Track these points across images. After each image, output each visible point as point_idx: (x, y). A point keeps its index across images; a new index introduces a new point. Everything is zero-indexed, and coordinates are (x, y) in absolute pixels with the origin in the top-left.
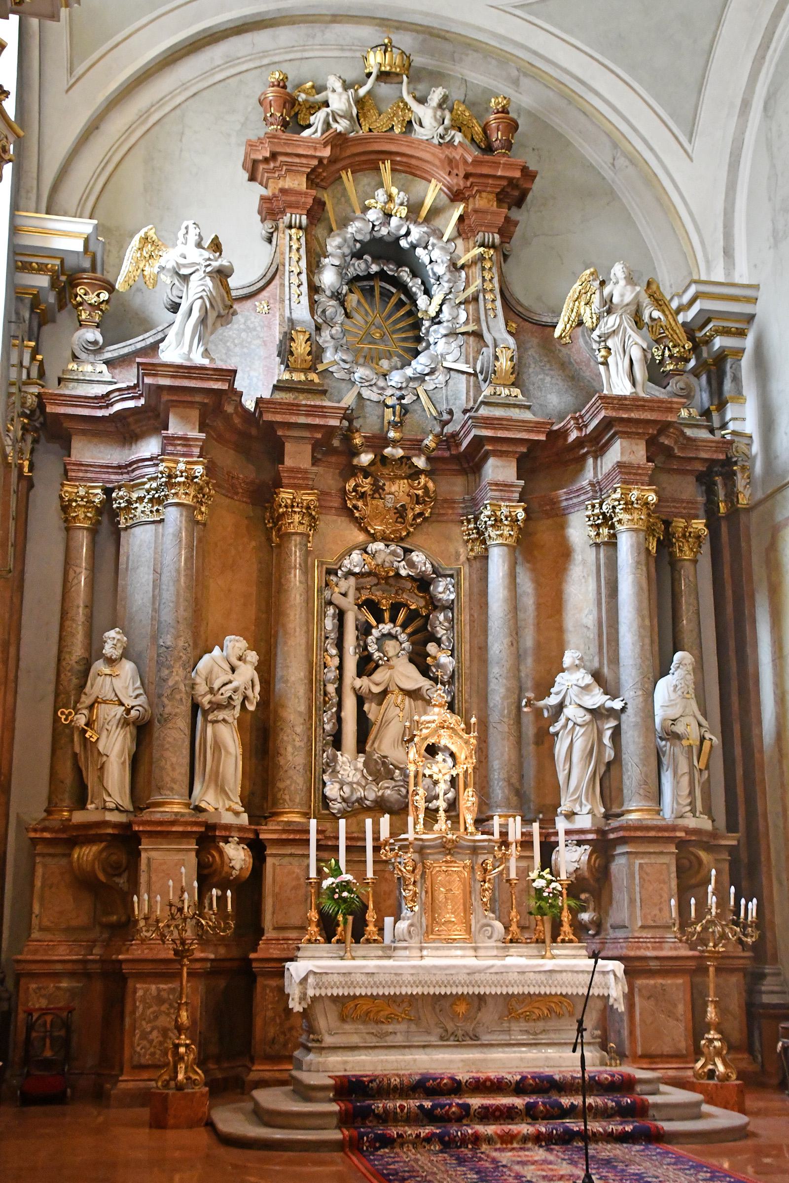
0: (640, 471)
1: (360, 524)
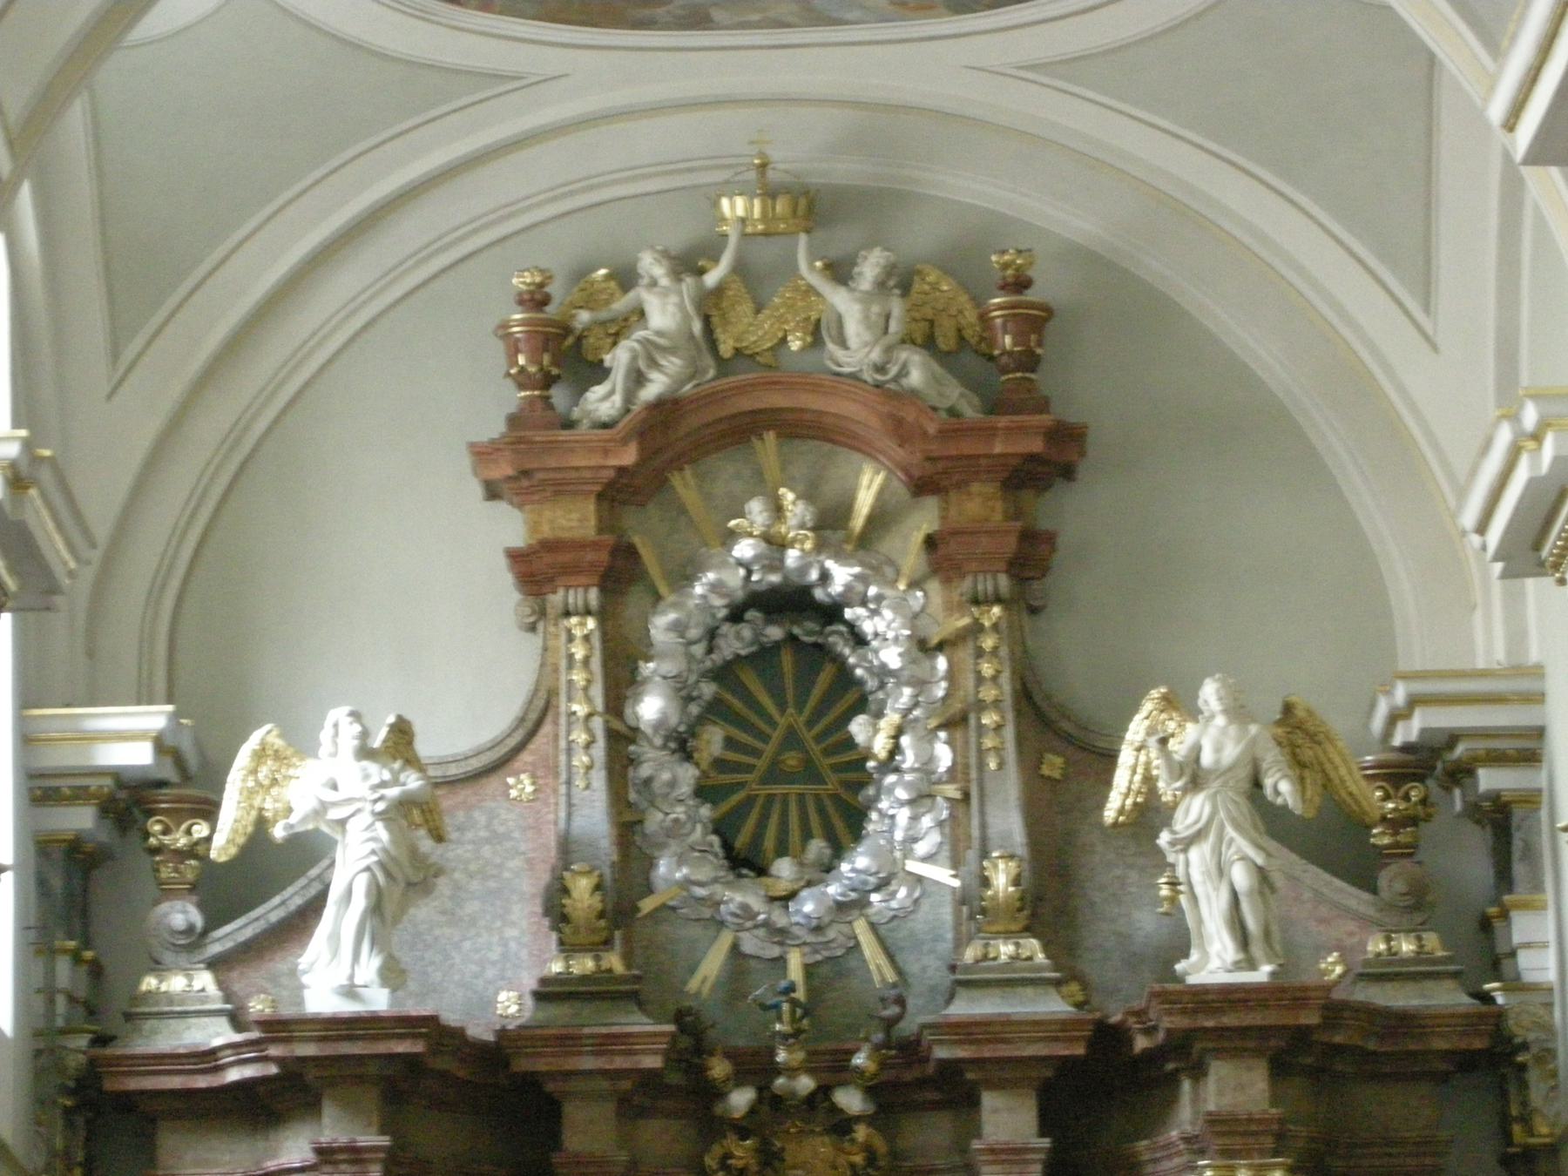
0: (1254, 1128)
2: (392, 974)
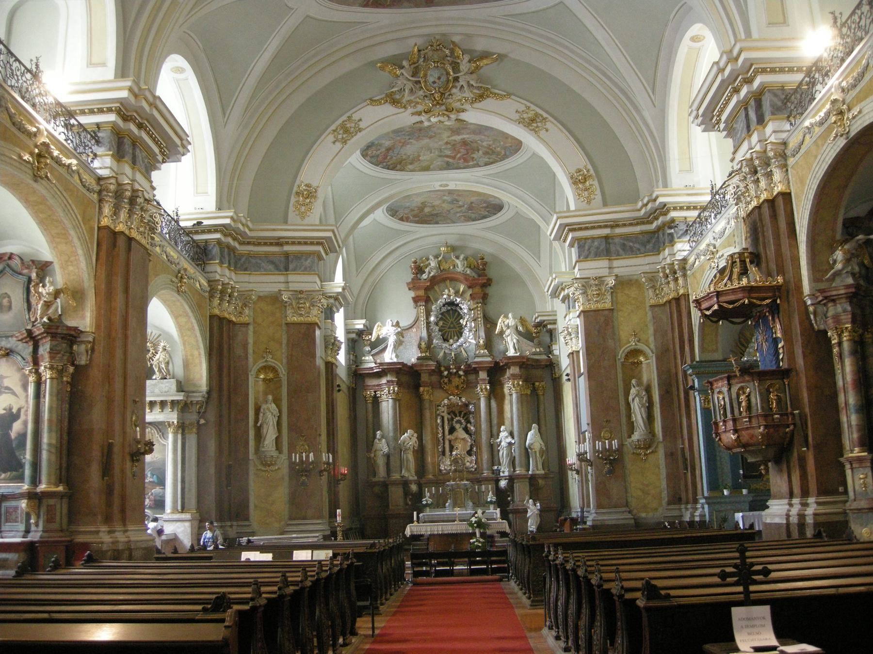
1: (446, 391)
2: (397, 356)
